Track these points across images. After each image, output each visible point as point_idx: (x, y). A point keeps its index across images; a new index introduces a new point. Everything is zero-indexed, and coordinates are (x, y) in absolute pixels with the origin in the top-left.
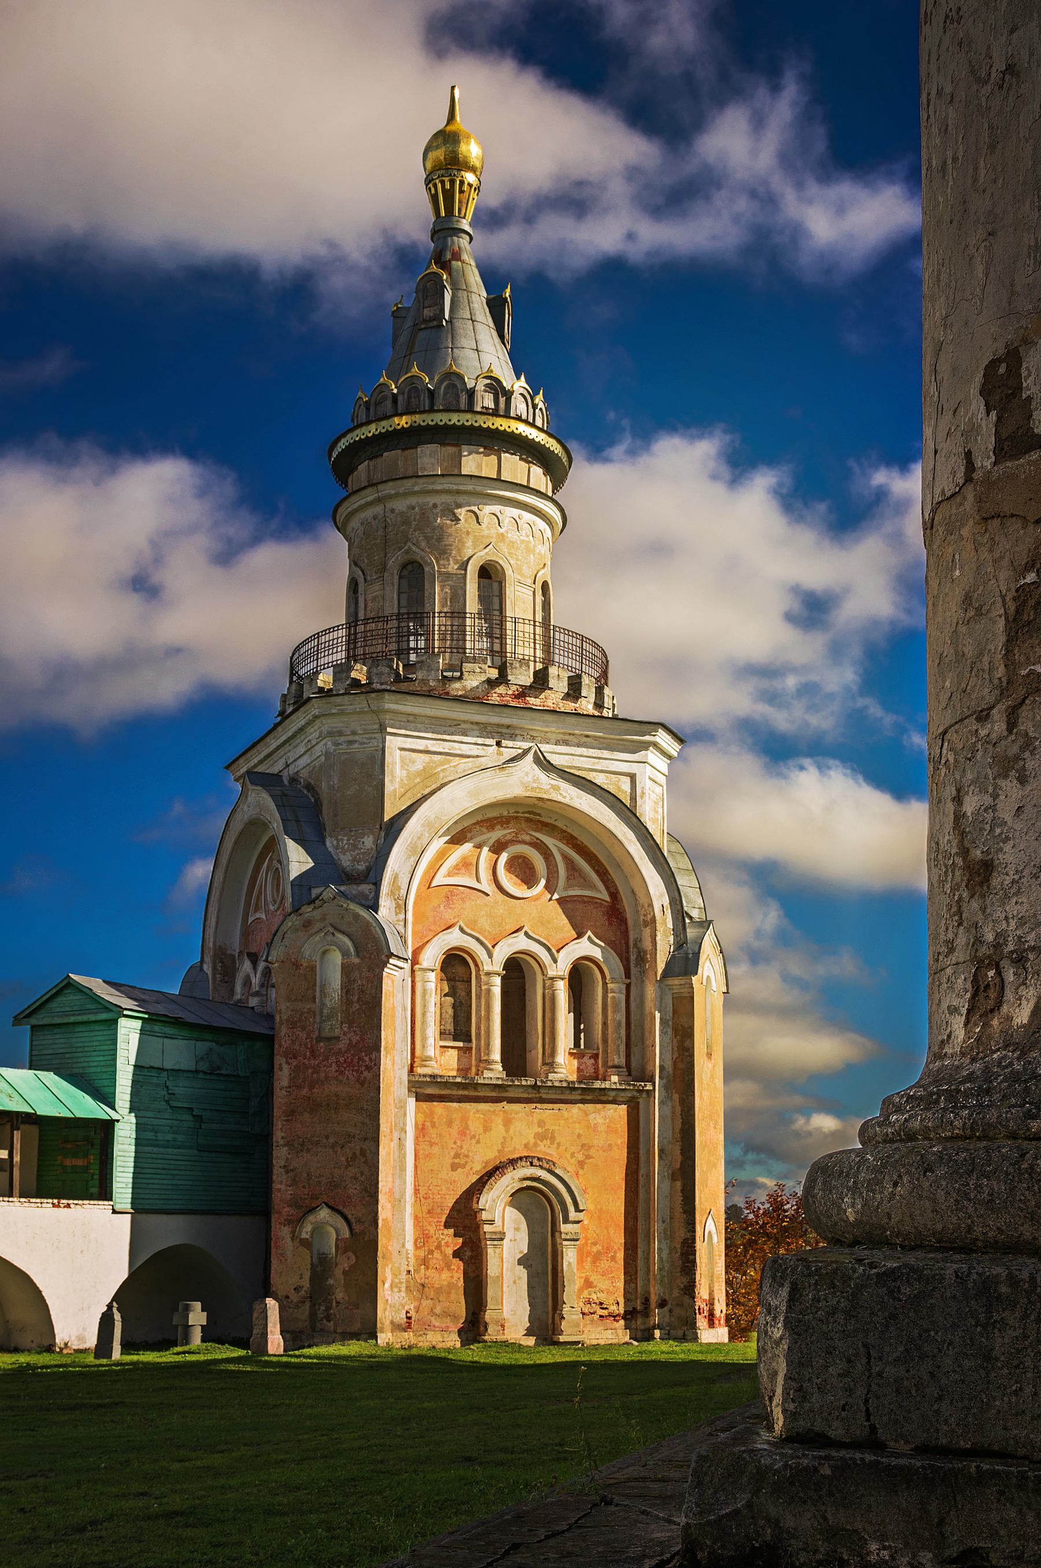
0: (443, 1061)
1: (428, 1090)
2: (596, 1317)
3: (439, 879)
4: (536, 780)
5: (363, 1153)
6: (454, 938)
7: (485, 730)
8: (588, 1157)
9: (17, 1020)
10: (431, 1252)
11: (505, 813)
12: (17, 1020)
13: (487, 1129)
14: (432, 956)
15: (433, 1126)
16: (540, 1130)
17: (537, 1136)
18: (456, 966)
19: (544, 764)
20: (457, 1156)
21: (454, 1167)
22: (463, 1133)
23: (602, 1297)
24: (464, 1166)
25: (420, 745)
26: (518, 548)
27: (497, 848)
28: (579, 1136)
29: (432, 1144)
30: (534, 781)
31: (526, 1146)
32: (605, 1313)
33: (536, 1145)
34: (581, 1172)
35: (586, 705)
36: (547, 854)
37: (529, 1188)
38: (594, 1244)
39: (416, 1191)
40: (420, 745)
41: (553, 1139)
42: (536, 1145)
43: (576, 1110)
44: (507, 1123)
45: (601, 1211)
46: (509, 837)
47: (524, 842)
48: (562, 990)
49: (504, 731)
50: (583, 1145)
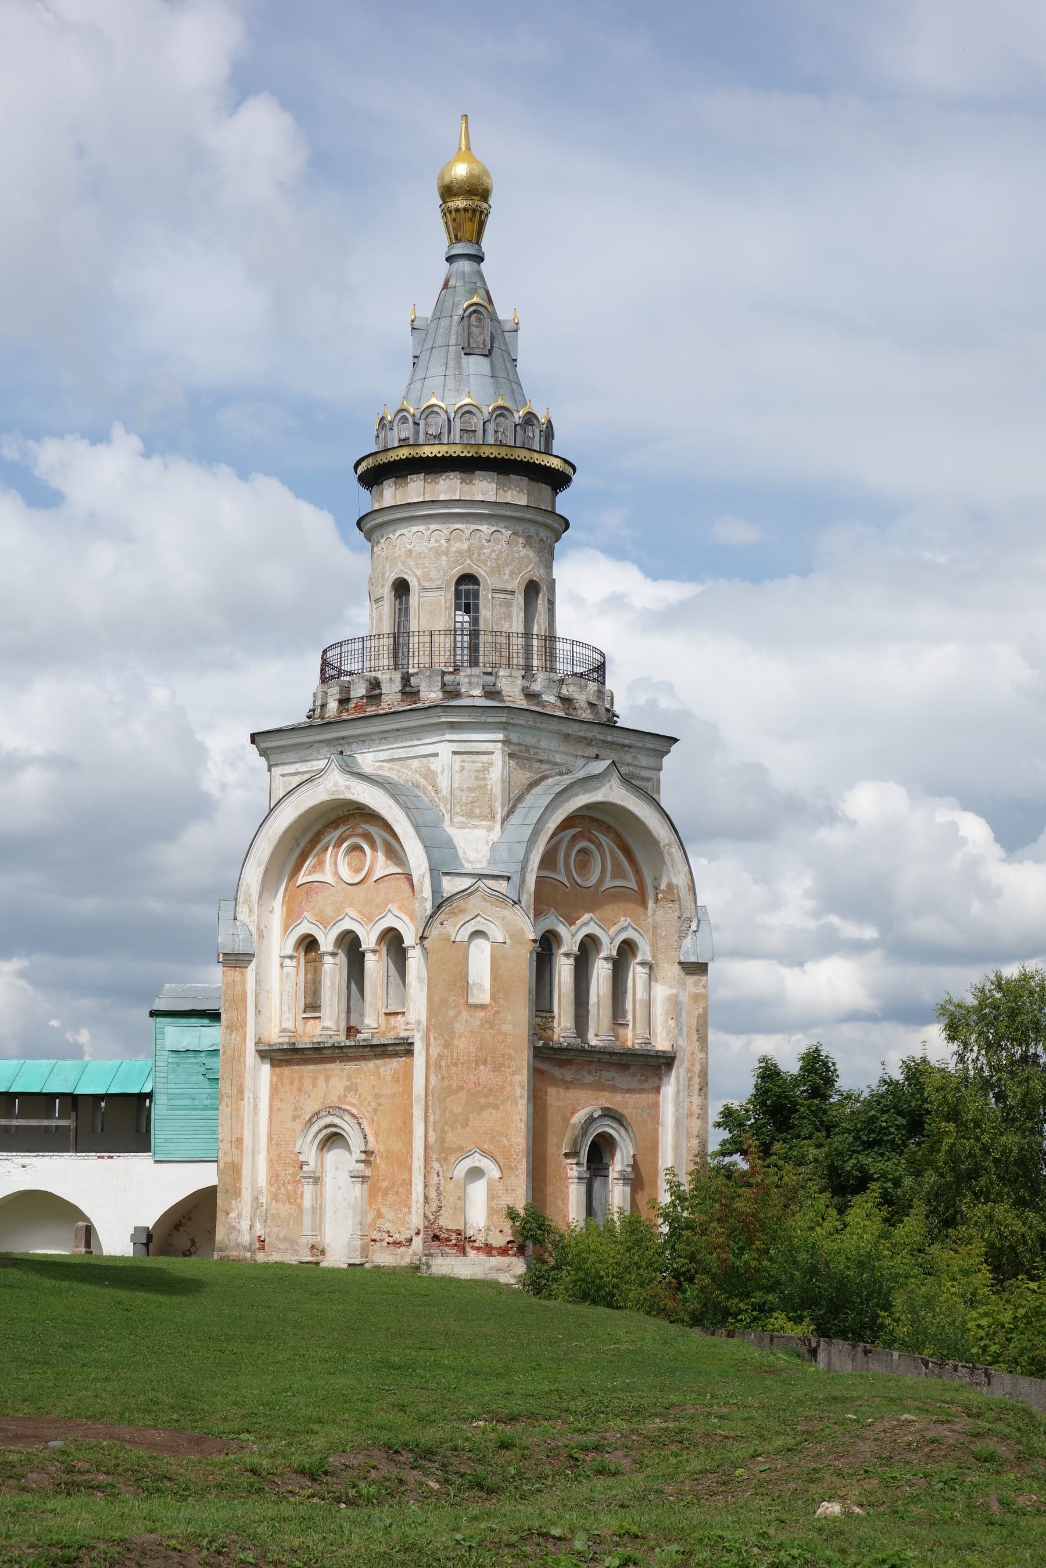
2: (385, 1244)
4: (336, 784)
8: (379, 1105)
10: (279, 1188)
11: (341, 814)
13: (314, 1085)
15: (282, 1086)
16: (348, 1084)
17: (348, 1089)
20: (296, 1109)
21: (295, 1118)
22: (300, 1090)
23: (387, 1226)
24: (298, 1117)
26: (425, 557)
28: (374, 1087)
29: (282, 1100)
30: (334, 785)
31: (339, 1097)
32: (391, 1240)
33: (345, 1096)
34: (375, 1118)
38: (384, 1180)
39: (270, 1139)
41: (356, 1090)
42: (345, 1096)
43: (371, 1064)
44: (327, 1079)
45: (388, 1151)
46: (348, 833)
47: (355, 835)
49: (342, 742)
50: (376, 1095)
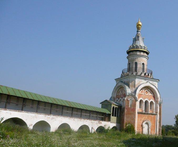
0: (140, 111)
1: (139, 113)
3: (140, 93)
5: (134, 119)
6: (141, 99)
7: (144, 79)
9: (100, 103)
12: (100, 103)
14: (139, 101)
18: (141, 101)
19: (149, 83)
25: (139, 80)
27: (145, 90)
35: (152, 77)
36: (148, 91)
37: (147, 123)
40: (139, 80)
48: (149, 104)
